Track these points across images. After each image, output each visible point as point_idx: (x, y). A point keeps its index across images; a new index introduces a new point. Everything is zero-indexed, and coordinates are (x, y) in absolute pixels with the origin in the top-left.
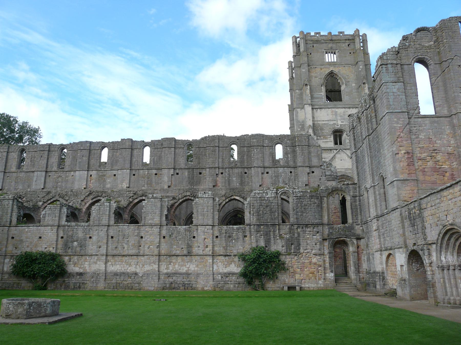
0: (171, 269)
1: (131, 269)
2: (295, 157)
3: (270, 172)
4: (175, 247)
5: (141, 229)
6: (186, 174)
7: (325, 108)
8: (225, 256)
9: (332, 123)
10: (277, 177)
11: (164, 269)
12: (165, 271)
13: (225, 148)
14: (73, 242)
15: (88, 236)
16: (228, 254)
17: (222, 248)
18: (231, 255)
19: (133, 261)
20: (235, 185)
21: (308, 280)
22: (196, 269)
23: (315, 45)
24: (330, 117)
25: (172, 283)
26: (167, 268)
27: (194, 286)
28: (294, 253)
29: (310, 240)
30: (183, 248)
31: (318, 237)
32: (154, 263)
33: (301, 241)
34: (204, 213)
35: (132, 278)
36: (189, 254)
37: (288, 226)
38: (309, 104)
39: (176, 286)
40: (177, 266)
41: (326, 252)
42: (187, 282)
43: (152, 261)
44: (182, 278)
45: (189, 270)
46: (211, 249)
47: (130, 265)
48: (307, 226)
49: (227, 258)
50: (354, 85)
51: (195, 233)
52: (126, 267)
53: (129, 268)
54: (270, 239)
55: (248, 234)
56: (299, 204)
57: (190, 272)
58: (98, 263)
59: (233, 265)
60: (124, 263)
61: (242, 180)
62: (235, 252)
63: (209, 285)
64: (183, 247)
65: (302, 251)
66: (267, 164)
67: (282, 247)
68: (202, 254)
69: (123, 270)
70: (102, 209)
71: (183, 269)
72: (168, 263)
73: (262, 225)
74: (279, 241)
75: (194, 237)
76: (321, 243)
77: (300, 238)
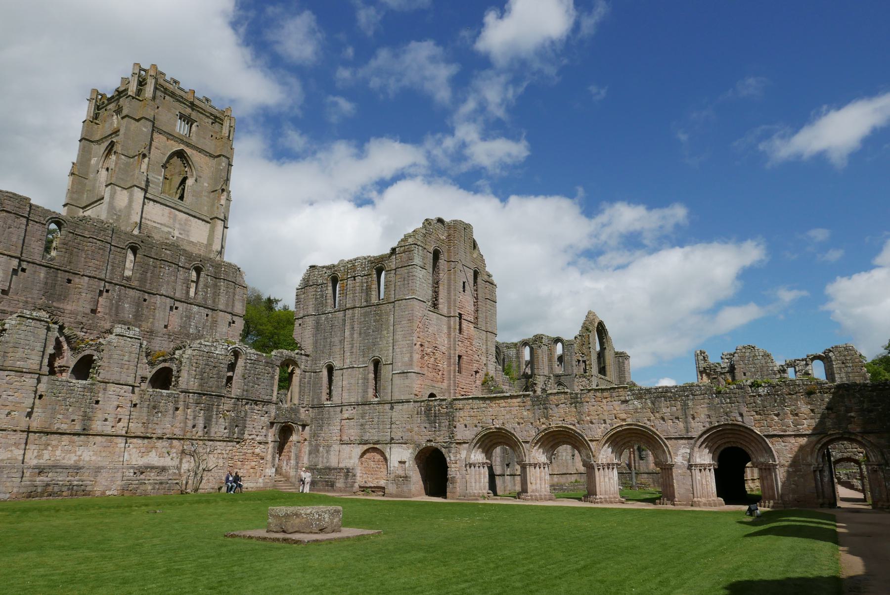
0: (47, 457)
2: (216, 295)
3: (180, 309)
4: (60, 416)
6: (42, 275)
7: (161, 204)
9: (166, 229)
10: (189, 317)
11: (32, 459)
12: (34, 462)
13: (119, 250)
16: (149, 435)
17: (141, 425)
18: (151, 438)
20: (126, 316)
22: (93, 458)
23: (167, 97)
24: (165, 220)
25: (48, 485)
26: (39, 457)
27: (88, 488)
30: (73, 421)
31: (265, 420)
32: (16, 445)
33: (248, 422)
34: (123, 362)
36: (85, 432)
38: (142, 189)
39: (56, 489)
40: (58, 453)
41: (270, 439)
42: (75, 483)
43: (13, 442)
44: (66, 474)
45: (79, 460)
46: (126, 425)
48: (256, 402)
49: (146, 441)
50: (206, 184)
51: (100, 395)
54: (211, 416)
57: (81, 464)
59: (153, 453)
61: (137, 311)
63: (114, 487)
64: (76, 417)
65: (246, 436)
66: (178, 295)
67: (225, 429)
68: (110, 433)
71: (70, 459)
72: (42, 447)
73: (204, 395)
74: (221, 420)
75: (97, 402)
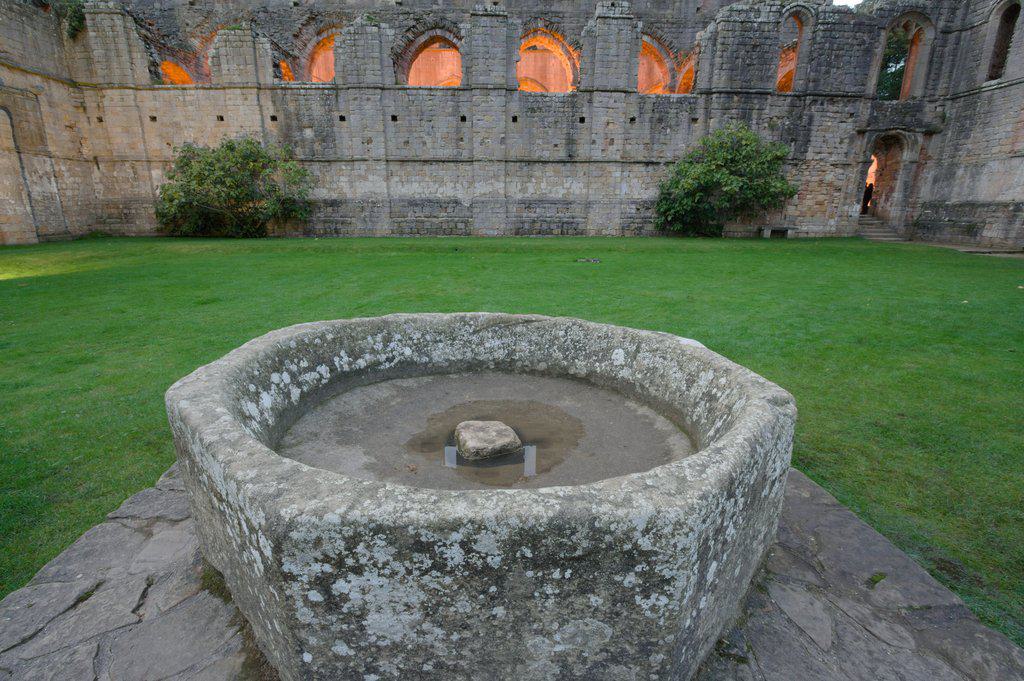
0: (532, 191)
1: (446, 192)
4: (540, 141)
5: (462, 99)
8: (647, 164)
12: (519, 196)
14: (301, 129)
15: (336, 115)
16: (654, 160)
17: (642, 147)
18: (658, 163)
19: (446, 172)
21: (808, 218)
26: (524, 190)
28: (792, 160)
29: (832, 132)
30: (556, 146)
31: (849, 127)
33: (813, 133)
35: (449, 210)
36: (571, 160)
37: (789, 100)
39: (545, 226)
40: (543, 185)
43: (491, 174)
44: (555, 210)
45: (568, 193)
47: (442, 183)
49: (650, 168)
51: (584, 109)
52: (433, 187)
53: (441, 190)
55: (700, 114)
56: (827, 45)
57: (571, 198)
58: (371, 178)
60: (427, 179)
62: (669, 155)
65: (810, 155)
68: (599, 158)
69: (426, 194)
70: (362, 42)
75: (582, 120)
76: (852, 139)
77: (812, 128)
